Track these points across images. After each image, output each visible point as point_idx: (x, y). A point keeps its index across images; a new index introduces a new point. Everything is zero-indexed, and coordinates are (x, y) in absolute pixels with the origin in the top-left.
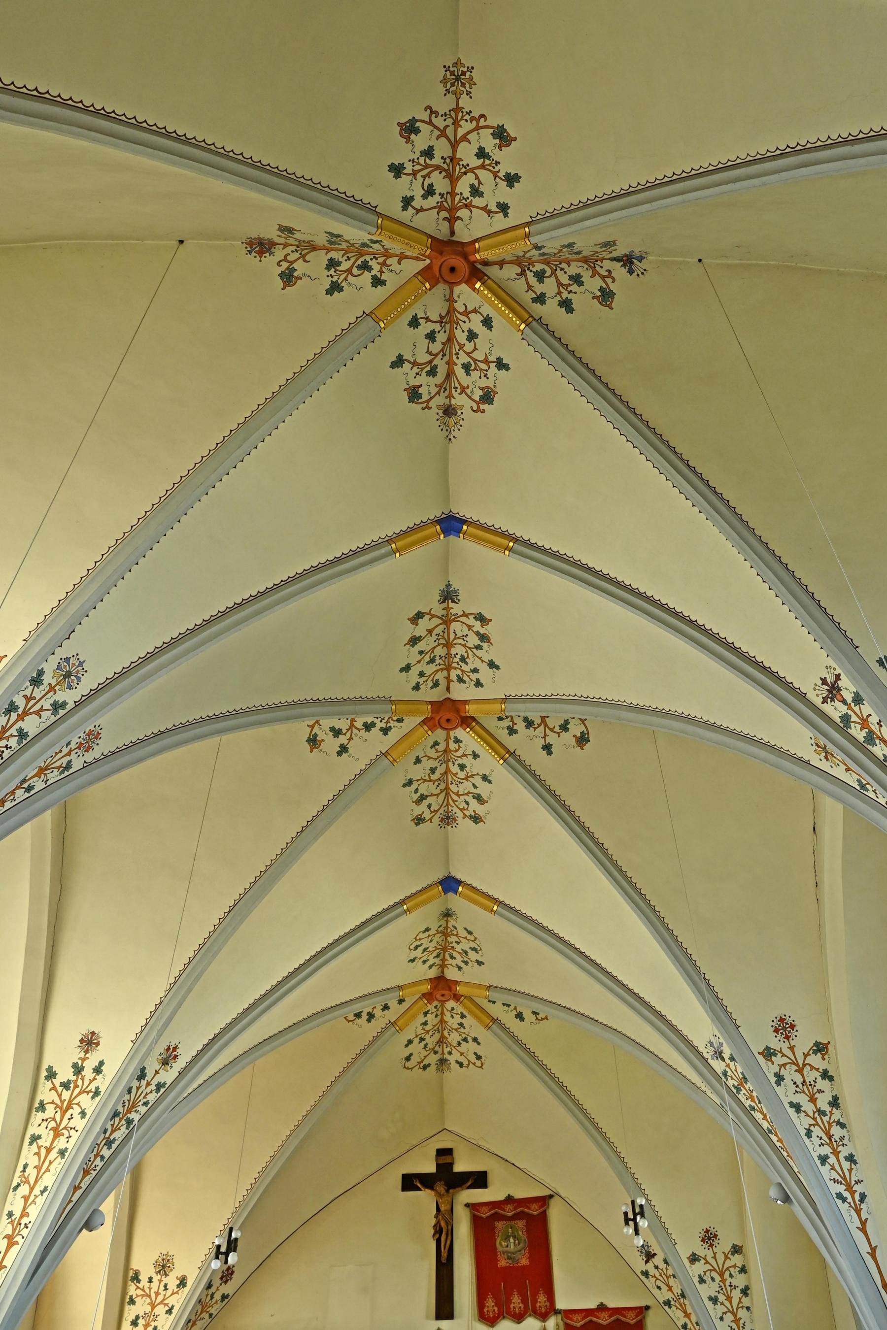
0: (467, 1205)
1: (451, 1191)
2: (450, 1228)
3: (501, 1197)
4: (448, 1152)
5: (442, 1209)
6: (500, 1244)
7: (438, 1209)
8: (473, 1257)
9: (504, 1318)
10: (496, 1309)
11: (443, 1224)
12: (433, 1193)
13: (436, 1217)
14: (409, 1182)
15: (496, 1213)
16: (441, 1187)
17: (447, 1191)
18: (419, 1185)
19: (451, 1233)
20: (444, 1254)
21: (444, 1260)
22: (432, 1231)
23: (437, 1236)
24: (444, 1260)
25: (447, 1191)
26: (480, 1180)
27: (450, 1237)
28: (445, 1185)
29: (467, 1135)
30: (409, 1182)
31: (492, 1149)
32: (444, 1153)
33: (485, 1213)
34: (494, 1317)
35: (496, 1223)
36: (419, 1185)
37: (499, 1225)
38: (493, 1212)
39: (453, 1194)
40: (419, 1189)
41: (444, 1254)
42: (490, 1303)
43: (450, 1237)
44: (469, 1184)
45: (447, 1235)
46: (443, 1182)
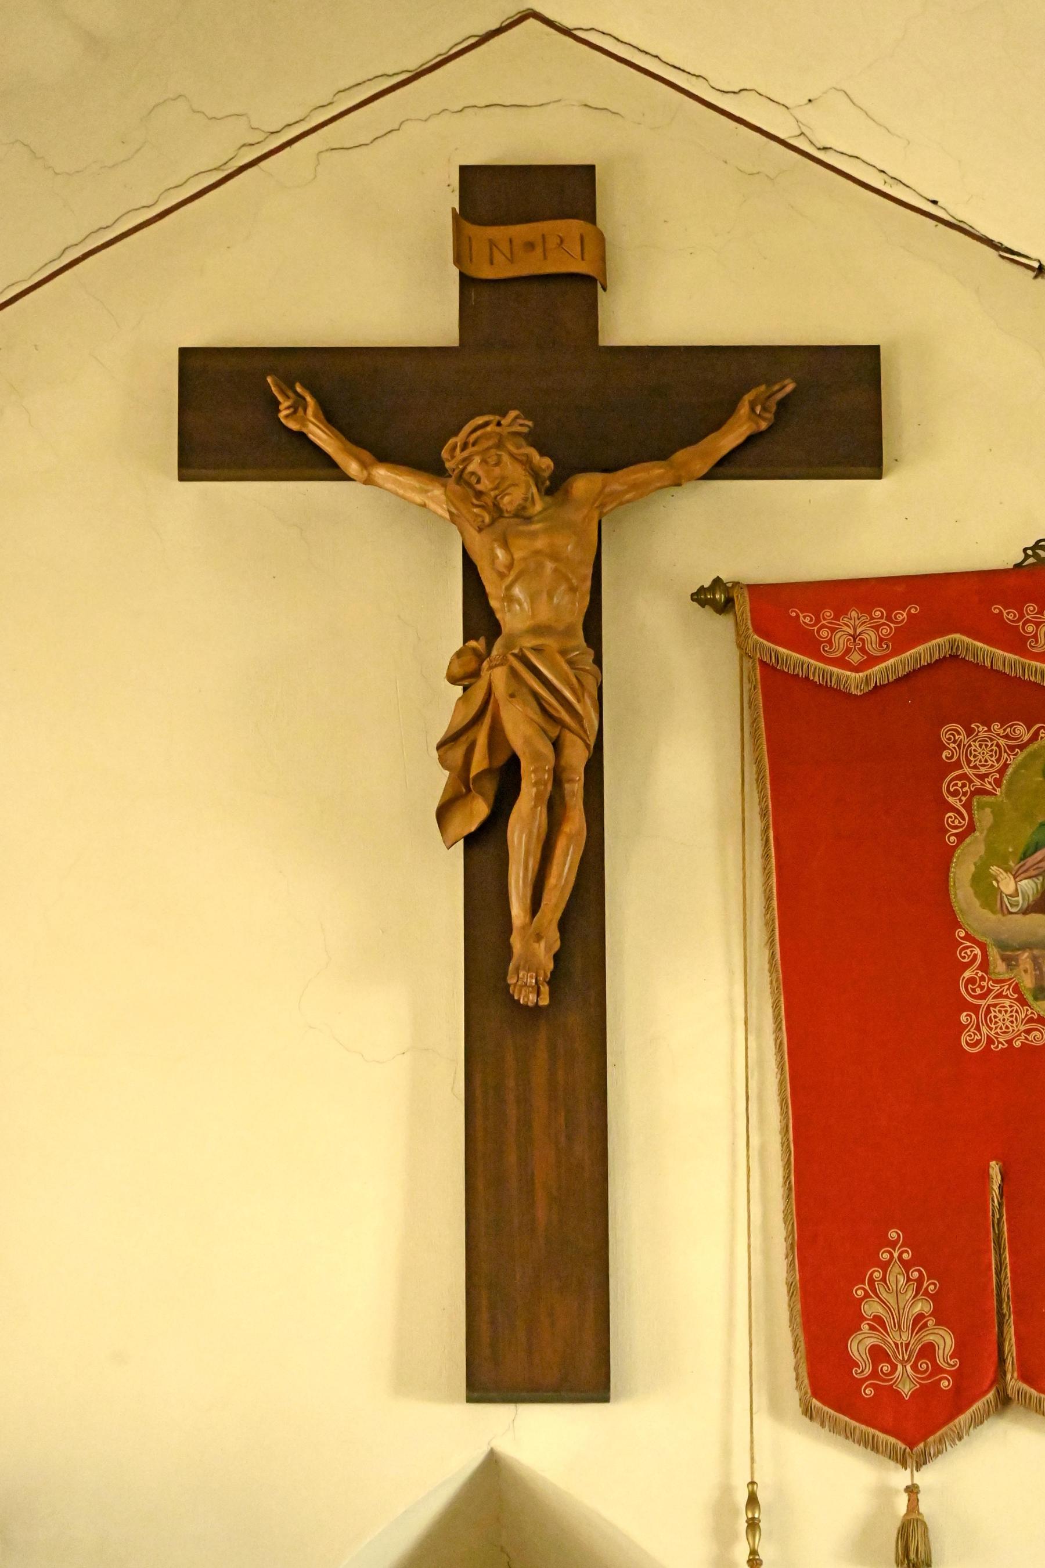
0: (716, 597)
1: (583, 485)
2: (577, 756)
3: (995, 547)
4: (565, 191)
5: (513, 619)
6: (989, 895)
7: (480, 618)
8: (760, 959)
9: (1004, 1402)
10: (944, 1341)
11: (520, 727)
12: (436, 497)
13: (464, 676)
14: (242, 414)
15: (952, 659)
16: (499, 454)
17: (554, 487)
18: (321, 436)
19: (586, 792)
20: (534, 947)
21: (528, 987)
22: (437, 781)
23: (480, 809)
24: (528, 987)
25: (554, 487)
26: (824, 410)
27: (575, 822)
28: (537, 440)
29: (719, 71)
30: (242, 414)
31: (925, 179)
32: (527, 210)
33: (860, 660)
34: (927, 1392)
35: (950, 733)
36: (321, 436)
37: (975, 748)
38: (924, 651)
39: (603, 505)
40: (328, 469)
41: (534, 947)
42: (896, 1301)
43: (575, 822)
44: (729, 438)
45: (555, 807)
46: (514, 421)
